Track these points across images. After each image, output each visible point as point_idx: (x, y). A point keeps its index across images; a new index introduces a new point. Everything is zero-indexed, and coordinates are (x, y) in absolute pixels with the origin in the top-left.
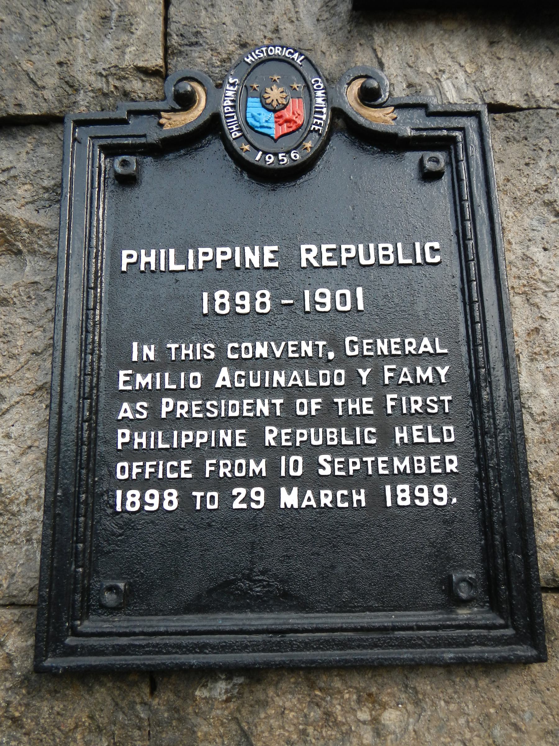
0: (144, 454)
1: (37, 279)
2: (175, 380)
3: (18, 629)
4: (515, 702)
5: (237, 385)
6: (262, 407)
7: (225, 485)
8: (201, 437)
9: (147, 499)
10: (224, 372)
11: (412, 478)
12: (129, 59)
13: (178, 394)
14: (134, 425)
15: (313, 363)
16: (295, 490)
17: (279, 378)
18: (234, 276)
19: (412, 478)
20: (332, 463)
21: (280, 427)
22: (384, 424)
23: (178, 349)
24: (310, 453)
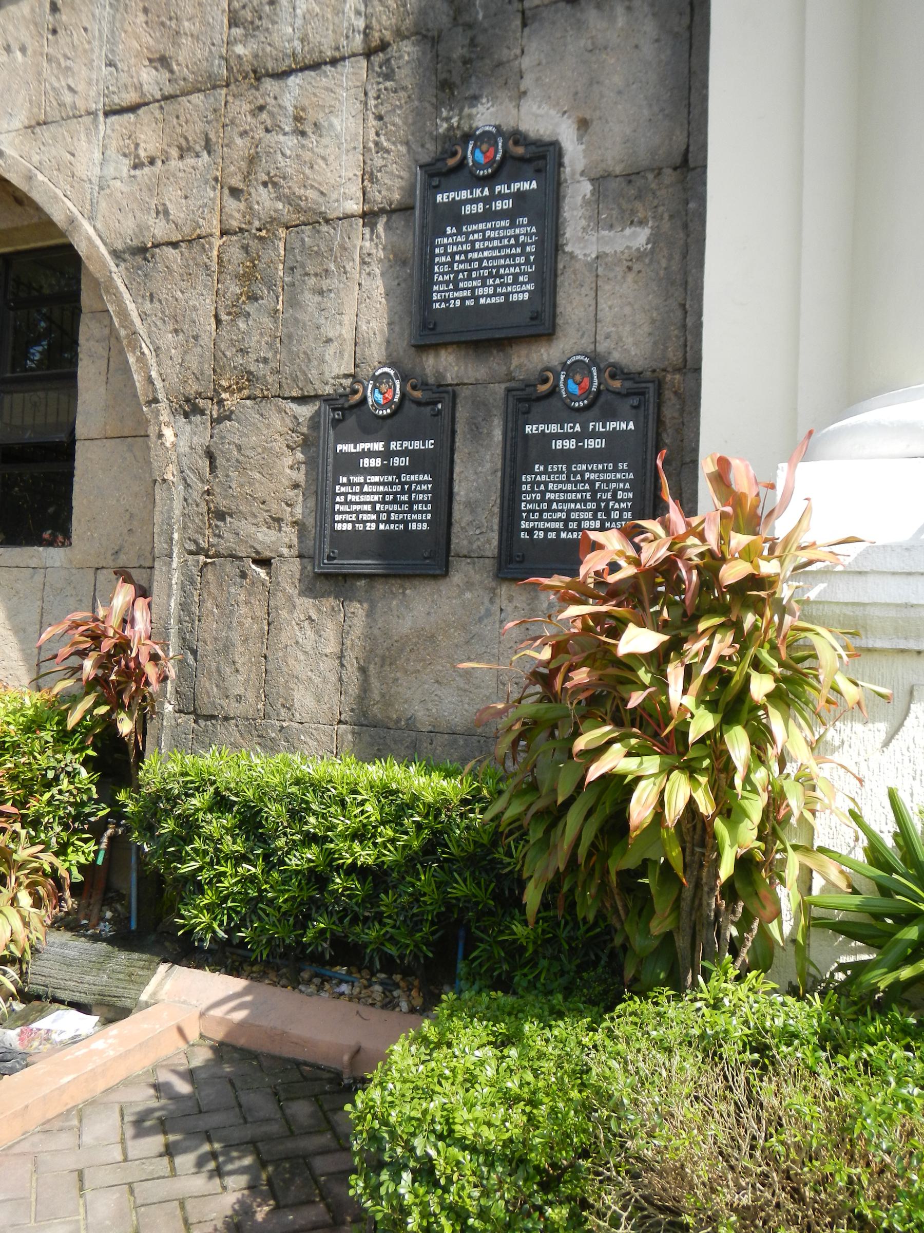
6: (376, 498)
7: (364, 522)
8: (358, 507)
11: (417, 521)
12: (341, 373)
15: (391, 484)
17: (381, 488)
18: (371, 454)
19: (417, 521)
22: (411, 503)
24: (389, 513)
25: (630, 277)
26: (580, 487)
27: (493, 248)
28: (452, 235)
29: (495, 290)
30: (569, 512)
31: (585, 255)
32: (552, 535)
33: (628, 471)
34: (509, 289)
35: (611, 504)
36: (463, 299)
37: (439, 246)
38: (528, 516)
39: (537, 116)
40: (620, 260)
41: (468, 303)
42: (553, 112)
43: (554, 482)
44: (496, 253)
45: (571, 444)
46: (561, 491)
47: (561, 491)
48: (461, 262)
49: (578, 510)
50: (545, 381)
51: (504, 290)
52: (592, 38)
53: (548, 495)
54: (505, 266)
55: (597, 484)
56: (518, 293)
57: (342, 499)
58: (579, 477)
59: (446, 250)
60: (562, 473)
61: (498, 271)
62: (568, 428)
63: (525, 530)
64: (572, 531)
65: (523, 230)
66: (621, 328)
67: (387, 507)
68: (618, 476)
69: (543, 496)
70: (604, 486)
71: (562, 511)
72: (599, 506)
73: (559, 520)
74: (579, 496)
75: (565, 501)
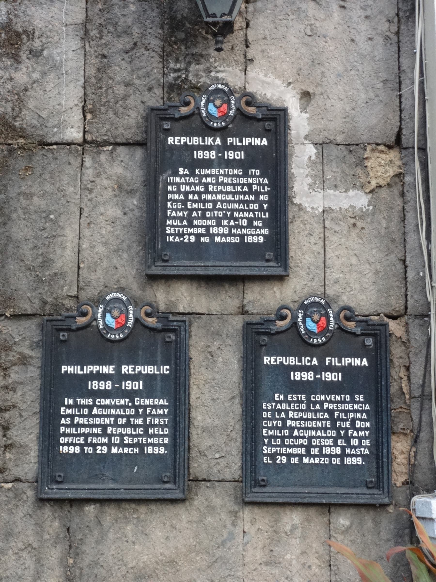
0: (69, 435)
1: (32, 375)
2: (79, 411)
3: (30, 489)
4: (180, 513)
5: (99, 413)
6: (107, 421)
7: (94, 446)
9: (70, 449)
10: (95, 409)
11: (153, 445)
13: (80, 416)
14: (66, 426)
16: (116, 447)
17: (113, 412)
18: (100, 377)
19: (153, 445)
20: (128, 439)
21: (113, 427)
22: (146, 427)
23: (80, 401)
24: (122, 436)
25: (354, 233)
26: (320, 415)
27: (227, 193)
28: (185, 176)
29: (230, 231)
30: (310, 438)
31: (312, 208)
33: (365, 403)
34: (244, 231)
35: (350, 432)
36: (198, 236)
37: (172, 184)
38: (270, 442)
39: (264, 82)
40: (344, 217)
41: (202, 239)
42: (278, 82)
43: (294, 411)
44: (230, 197)
45: (309, 376)
46: (301, 419)
47: (301, 419)
48: (195, 201)
49: (319, 437)
50: (283, 318)
51: (239, 232)
52: (311, 25)
53: (289, 423)
54: (239, 211)
55: (336, 414)
56: (253, 235)
57: (69, 421)
58: (318, 407)
59: (179, 188)
60: (303, 402)
61: (232, 214)
62: (305, 361)
63: (267, 455)
64: (315, 456)
65: (256, 180)
66: (348, 276)
67: (119, 430)
68: (356, 407)
69: (284, 423)
70: (343, 416)
71: (304, 437)
72: (339, 433)
73: (302, 446)
74: (319, 424)
75: (307, 429)
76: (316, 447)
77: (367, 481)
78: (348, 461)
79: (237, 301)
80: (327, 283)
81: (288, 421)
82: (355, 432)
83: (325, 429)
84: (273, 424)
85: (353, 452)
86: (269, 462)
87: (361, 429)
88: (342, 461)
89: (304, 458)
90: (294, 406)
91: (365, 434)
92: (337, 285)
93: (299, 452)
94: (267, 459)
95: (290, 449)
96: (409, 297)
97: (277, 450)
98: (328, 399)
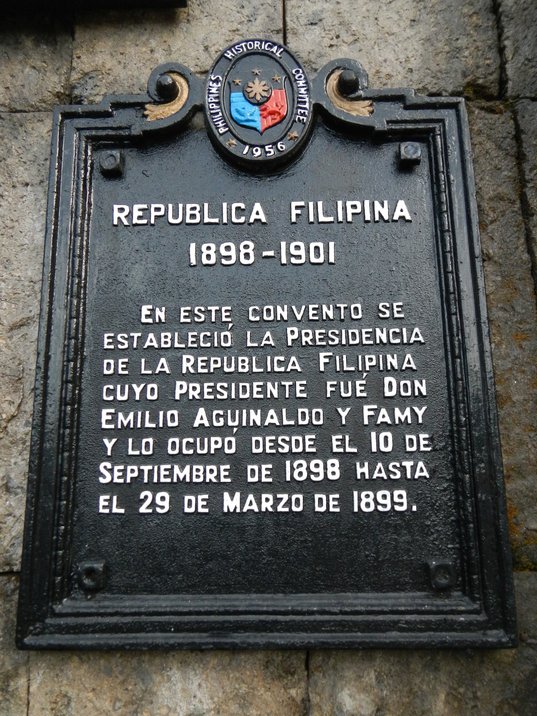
30: (246, 432)
32: (196, 504)
43: (198, 351)
45: (242, 252)
47: (219, 375)
49: (272, 429)
50: (167, 94)
63: (111, 487)
64: (259, 488)
72: (332, 418)
73: (218, 457)
74: (273, 390)
76: (263, 458)
77: (426, 567)
78: (364, 502)
79: (55, 79)
80: (290, 24)
81: (178, 383)
82: (383, 411)
83: (290, 403)
84: (132, 391)
85: (379, 473)
86: (115, 510)
87: (400, 401)
88: (346, 501)
89: (226, 495)
90: (197, 337)
91: (414, 414)
92: (317, 29)
93: (211, 477)
94: (110, 501)
95: (182, 468)
96: (509, 53)
97: (141, 472)
98: (299, 317)
